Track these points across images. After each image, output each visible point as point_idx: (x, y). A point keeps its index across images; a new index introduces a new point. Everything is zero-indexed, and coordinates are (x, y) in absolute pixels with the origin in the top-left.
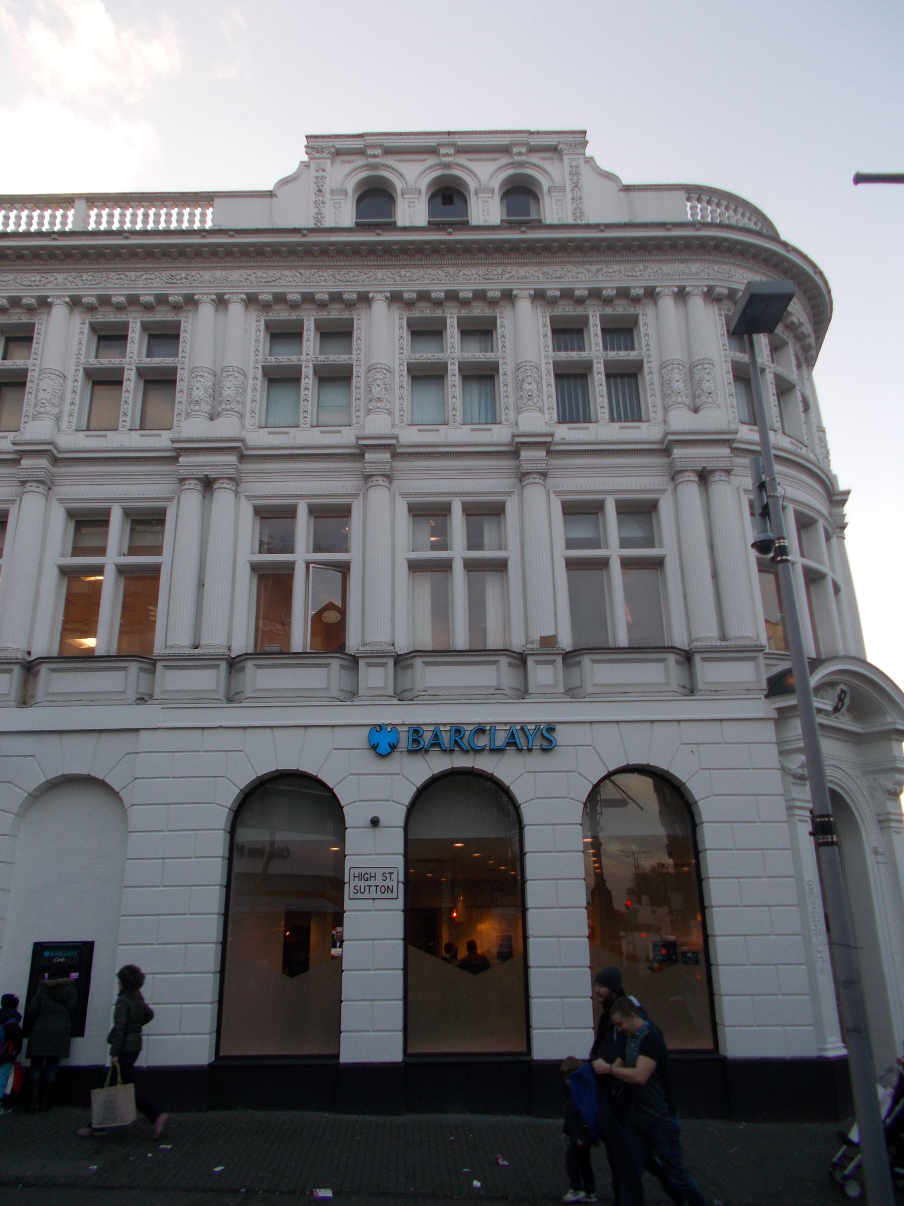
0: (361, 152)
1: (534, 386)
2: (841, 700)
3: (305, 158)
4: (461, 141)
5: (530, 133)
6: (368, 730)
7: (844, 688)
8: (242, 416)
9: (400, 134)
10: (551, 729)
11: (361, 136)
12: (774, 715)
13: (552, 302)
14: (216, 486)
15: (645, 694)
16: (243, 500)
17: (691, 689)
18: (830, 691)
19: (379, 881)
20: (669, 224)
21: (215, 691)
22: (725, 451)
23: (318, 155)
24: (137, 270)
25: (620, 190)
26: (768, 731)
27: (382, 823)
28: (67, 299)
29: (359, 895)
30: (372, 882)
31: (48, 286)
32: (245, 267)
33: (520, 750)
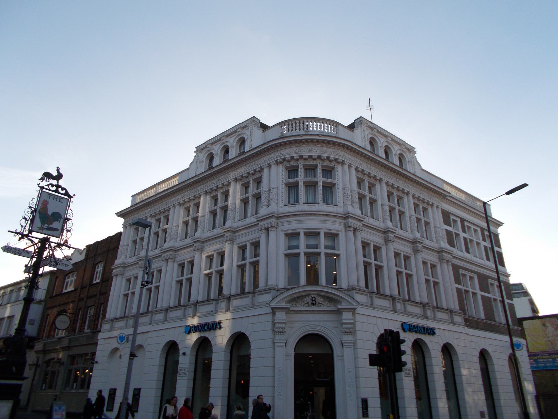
0: (206, 147)
1: (230, 212)
2: (312, 300)
3: (195, 154)
4: (225, 134)
5: (241, 123)
6: (184, 327)
8: (177, 238)
9: (213, 138)
10: (221, 322)
11: (205, 143)
12: (271, 311)
13: (240, 180)
14: (169, 261)
15: (242, 309)
16: (175, 263)
17: (253, 305)
18: (307, 298)
19: (184, 372)
20: (259, 146)
21: (162, 319)
22: (273, 220)
23: (197, 153)
24: (161, 203)
25: (262, 132)
26: (270, 317)
27: (186, 354)
28: (150, 216)
29: (180, 375)
30: (182, 372)
31: (148, 213)
32: (178, 195)
33: (214, 330)
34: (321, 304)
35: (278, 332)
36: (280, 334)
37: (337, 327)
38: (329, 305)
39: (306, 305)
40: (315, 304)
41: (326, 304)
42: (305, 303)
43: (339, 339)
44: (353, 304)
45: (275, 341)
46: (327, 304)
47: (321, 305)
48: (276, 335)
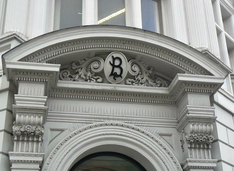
2: (113, 66)
7: (115, 55)
12: (7, 85)
18: (102, 61)
34: (133, 77)
35: (23, 134)
36: (28, 141)
37: (170, 135)
38: (150, 82)
39: (96, 79)
40: (120, 76)
41: (144, 79)
42: (96, 74)
43: (177, 161)
44: (212, 75)
45: (11, 158)
46: (147, 81)
47: (132, 82)
48: (15, 143)
